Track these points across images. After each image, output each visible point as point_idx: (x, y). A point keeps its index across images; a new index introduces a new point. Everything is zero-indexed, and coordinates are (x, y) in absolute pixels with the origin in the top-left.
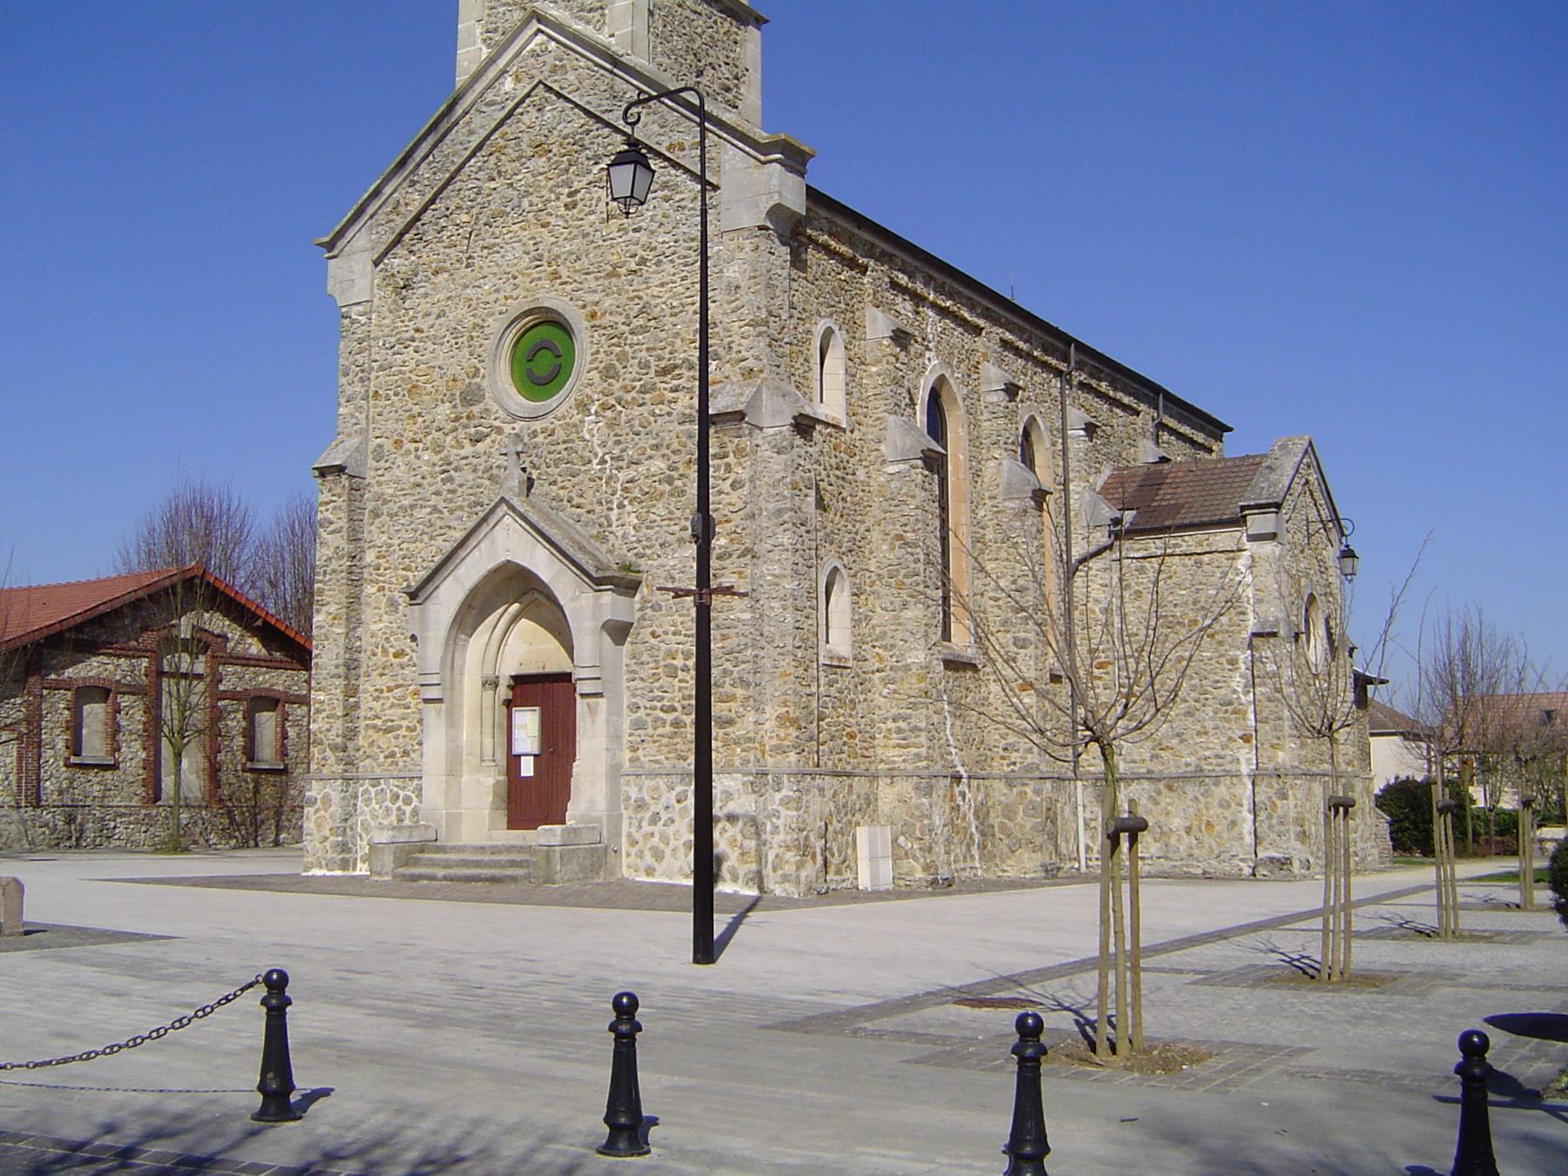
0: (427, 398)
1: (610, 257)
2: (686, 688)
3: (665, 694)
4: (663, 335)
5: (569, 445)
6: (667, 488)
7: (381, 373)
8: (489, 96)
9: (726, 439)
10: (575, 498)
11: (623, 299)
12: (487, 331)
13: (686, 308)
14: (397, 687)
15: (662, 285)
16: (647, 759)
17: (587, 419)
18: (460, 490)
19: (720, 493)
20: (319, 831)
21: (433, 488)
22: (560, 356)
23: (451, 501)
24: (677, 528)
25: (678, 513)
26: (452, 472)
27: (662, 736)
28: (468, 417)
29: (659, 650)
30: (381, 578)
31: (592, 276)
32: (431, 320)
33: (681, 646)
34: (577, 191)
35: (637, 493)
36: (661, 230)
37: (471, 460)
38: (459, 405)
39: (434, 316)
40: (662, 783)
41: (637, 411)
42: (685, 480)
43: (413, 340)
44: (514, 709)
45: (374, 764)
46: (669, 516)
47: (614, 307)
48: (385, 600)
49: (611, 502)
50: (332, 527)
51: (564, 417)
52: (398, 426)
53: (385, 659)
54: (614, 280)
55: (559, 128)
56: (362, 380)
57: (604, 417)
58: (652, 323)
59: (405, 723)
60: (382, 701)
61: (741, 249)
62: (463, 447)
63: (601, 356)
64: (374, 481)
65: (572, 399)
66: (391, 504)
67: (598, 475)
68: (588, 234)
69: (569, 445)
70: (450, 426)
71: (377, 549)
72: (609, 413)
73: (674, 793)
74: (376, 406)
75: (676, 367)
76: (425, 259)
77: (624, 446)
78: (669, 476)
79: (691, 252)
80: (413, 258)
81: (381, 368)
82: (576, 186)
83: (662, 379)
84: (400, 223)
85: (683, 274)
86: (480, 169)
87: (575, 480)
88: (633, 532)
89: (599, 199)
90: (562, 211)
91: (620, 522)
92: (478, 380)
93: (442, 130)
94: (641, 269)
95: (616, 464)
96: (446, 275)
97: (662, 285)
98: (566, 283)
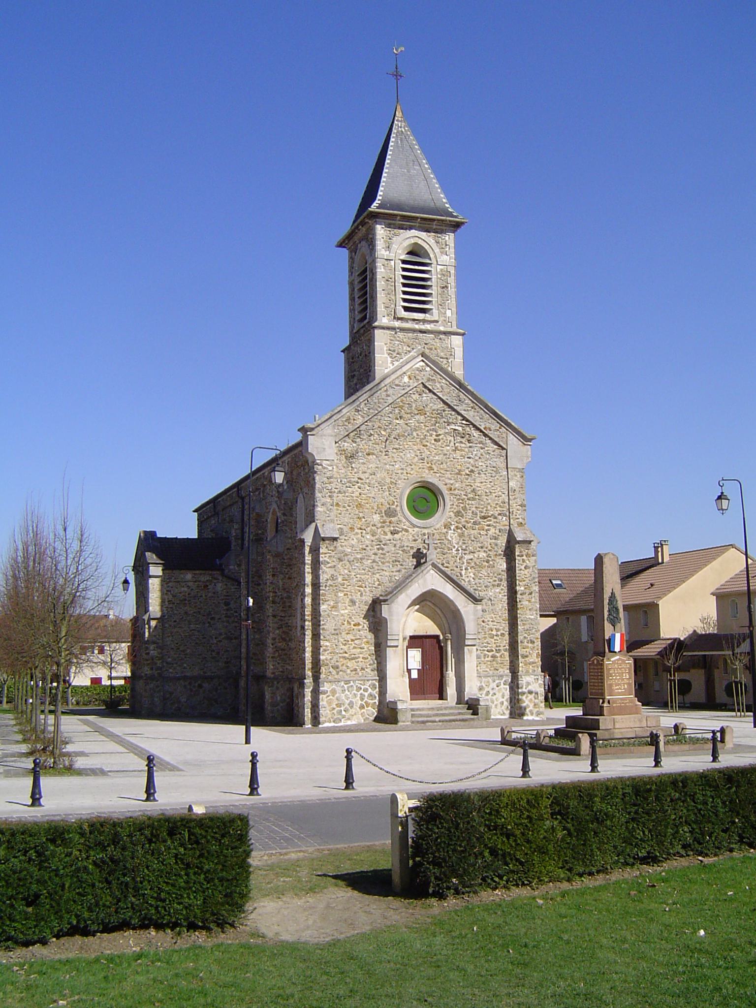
0: (366, 510)
4: (482, 503)
6: (487, 564)
8: (397, 382)
11: (464, 485)
14: (356, 639)
15: (482, 483)
19: (521, 570)
20: (329, 706)
21: (373, 552)
23: (383, 558)
25: (491, 575)
32: (367, 475)
34: (440, 435)
35: (473, 564)
40: (490, 680)
41: (473, 532)
50: (329, 565)
52: (351, 521)
54: (459, 476)
55: (431, 405)
56: (330, 496)
59: (361, 655)
60: (348, 646)
61: (516, 476)
63: (455, 506)
66: (349, 556)
68: (446, 454)
70: (380, 525)
72: (459, 531)
73: (495, 683)
74: (338, 510)
75: (489, 517)
76: (361, 446)
80: (354, 445)
82: (440, 433)
84: (351, 427)
86: (391, 413)
87: (445, 556)
89: (450, 441)
90: (433, 442)
92: (394, 507)
93: (373, 391)
96: (374, 457)
97: (482, 483)
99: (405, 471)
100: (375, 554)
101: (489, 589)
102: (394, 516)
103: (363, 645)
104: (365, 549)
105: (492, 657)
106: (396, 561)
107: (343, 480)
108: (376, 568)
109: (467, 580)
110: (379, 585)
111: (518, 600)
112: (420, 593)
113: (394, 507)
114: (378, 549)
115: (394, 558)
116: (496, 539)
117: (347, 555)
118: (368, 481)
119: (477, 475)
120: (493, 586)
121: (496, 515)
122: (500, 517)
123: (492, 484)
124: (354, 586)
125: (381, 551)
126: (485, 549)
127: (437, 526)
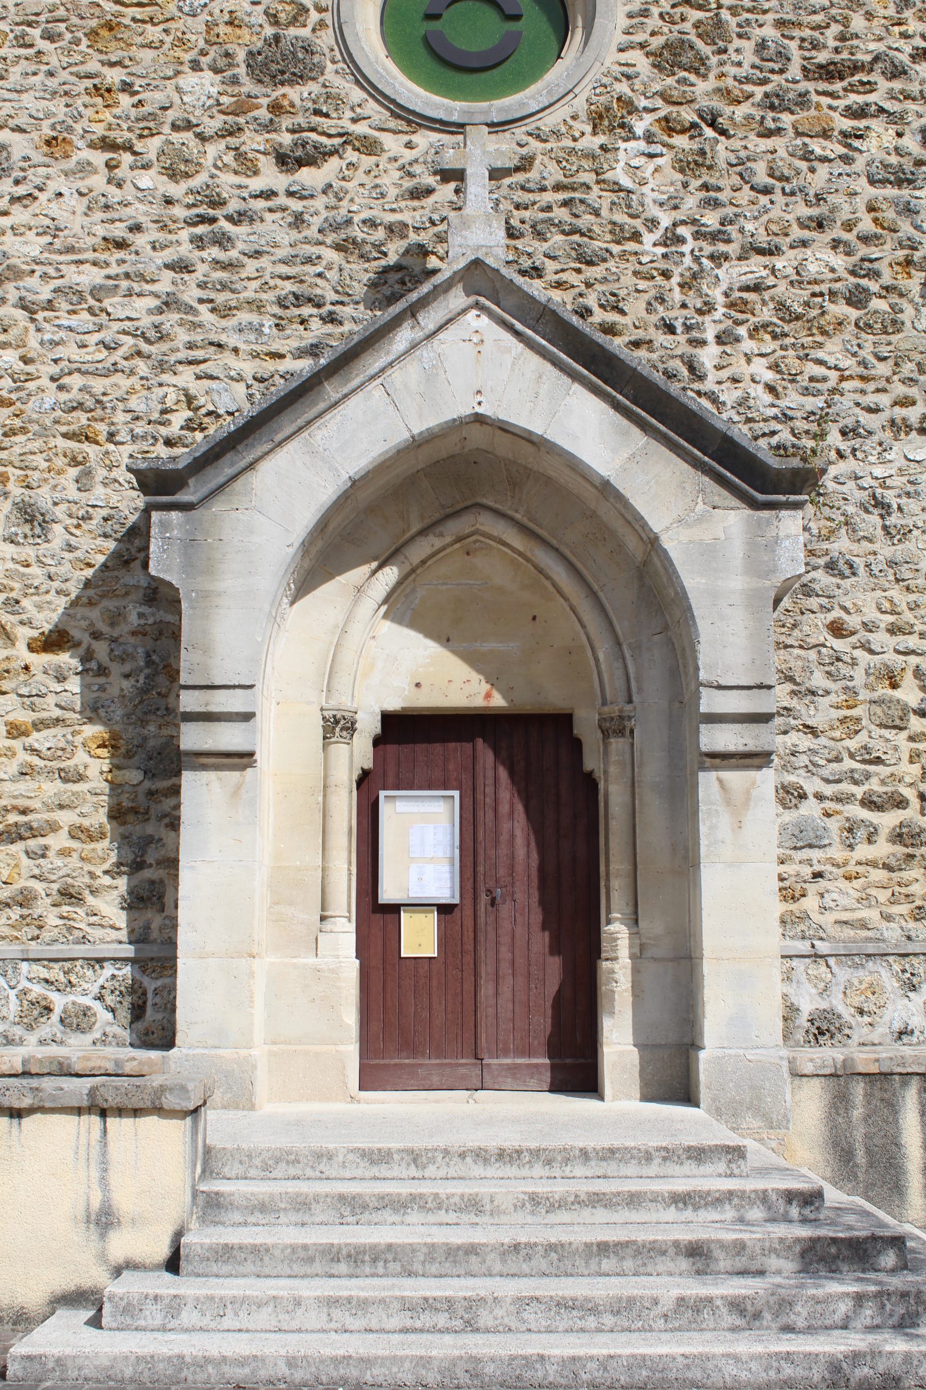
0: (148, 54)
3: (872, 768)
5: (577, 195)
6: (853, 314)
10: (596, 309)
14: (39, 725)
17: (622, 145)
18: (251, 266)
21: (168, 255)
22: (517, 17)
23: (224, 286)
24: (884, 400)
25: (883, 369)
26: (224, 224)
27: (873, 864)
28: (276, 108)
29: (854, 663)
37: (282, 200)
38: (244, 79)
42: (894, 299)
44: (382, 794)
46: (861, 370)
49: (699, 327)
51: (557, 134)
52: (58, 108)
59: (66, 818)
62: (256, 173)
63: (653, 22)
65: (582, 99)
66: (32, 282)
67: (662, 265)
69: (577, 195)
70: (212, 125)
72: (681, 141)
75: (856, 68)
77: (730, 211)
78: (857, 286)
83: (823, 86)
88: (768, 398)
91: (724, 374)
95: (708, 249)
100: (181, 267)
102: (300, 78)
103: (81, 757)
104: (121, 245)
105: (898, 837)
106: (299, 299)
108: (182, 336)
109: (729, 396)
110: (189, 426)
112: (401, 436)
113: (305, 32)
114: (199, 242)
115: (289, 287)
120: (898, 427)
121: (904, 58)
124: (44, 433)
125: (214, 252)
126: (837, 232)
127: (550, 121)
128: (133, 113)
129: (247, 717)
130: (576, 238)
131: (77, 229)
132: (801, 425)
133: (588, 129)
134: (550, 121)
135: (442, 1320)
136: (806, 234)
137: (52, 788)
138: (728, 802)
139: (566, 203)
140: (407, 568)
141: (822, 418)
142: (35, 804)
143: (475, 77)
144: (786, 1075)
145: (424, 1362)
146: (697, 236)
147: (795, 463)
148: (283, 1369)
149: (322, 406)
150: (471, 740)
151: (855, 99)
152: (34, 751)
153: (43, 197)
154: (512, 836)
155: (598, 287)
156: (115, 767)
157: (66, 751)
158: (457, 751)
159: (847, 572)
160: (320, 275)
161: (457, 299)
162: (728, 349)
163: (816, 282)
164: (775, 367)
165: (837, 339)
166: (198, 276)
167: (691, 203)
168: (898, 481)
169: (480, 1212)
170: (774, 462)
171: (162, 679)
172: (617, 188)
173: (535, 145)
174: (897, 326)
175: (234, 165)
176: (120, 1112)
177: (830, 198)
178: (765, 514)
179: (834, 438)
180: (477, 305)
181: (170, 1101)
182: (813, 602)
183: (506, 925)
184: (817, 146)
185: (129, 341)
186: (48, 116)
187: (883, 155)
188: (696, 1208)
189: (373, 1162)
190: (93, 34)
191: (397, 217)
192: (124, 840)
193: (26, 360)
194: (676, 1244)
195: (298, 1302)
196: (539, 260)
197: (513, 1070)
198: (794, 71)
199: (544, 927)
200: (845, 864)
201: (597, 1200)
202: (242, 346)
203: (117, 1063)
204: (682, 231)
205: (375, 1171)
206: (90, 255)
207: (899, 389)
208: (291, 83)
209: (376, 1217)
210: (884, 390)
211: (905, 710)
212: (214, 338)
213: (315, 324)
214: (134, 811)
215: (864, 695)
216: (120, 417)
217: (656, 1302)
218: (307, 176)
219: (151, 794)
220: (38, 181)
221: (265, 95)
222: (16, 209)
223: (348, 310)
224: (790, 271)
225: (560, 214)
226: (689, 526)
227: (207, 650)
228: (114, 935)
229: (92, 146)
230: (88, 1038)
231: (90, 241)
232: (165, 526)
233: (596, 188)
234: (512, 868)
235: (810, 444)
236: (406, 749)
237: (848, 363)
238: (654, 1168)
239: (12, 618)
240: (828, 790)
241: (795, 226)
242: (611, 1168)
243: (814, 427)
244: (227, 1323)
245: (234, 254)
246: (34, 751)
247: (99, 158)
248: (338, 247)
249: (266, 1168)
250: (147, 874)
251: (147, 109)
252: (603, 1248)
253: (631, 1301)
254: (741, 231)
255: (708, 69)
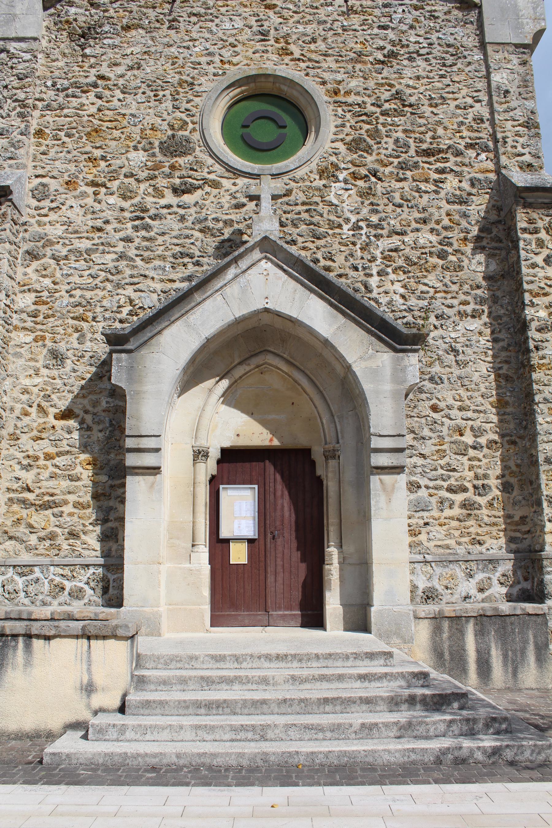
0: (114, 143)
1: (353, 45)
2: (480, 467)
3: (451, 473)
4: (422, 121)
5: (312, 207)
6: (441, 262)
7: (48, 112)
9: (535, 216)
10: (321, 259)
11: (371, 84)
12: (197, 88)
13: (448, 102)
14: (59, 454)
15: (418, 78)
16: (431, 544)
17: (333, 185)
18: (160, 240)
21: (122, 234)
22: (285, 127)
23: (148, 249)
24: (455, 302)
25: (455, 288)
27: (452, 518)
29: (443, 424)
30: (39, 327)
31: (332, 58)
32: (120, 70)
33: (470, 423)
35: (401, 262)
36: (413, 32)
37: (175, 209)
38: (158, 154)
39: (125, 67)
40: (459, 571)
42: (459, 256)
43: (95, 86)
45: (19, 546)
46: (444, 288)
47: (360, 89)
48: (45, 351)
49: (369, 268)
51: (303, 179)
52: (72, 168)
53: (41, 421)
54: (358, 66)
56: (21, 115)
57: (355, 186)
58: (406, 109)
59: (71, 498)
60: (35, 471)
62: (163, 197)
63: (347, 130)
64: (33, 221)
66: (58, 247)
67: (352, 239)
68: (325, 22)
69: (312, 207)
71: (34, 295)
72: (360, 183)
74: (39, 145)
75: (440, 151)
77: (383, 215)
78: (442, 250)
79: (448, 55)
81: (48, 107)
83: (425, 159)
85: (441, 73)
88: (401, 301)
91: (381, 290)
94: (391, 62)
95: (373, 232)
98: (299, 60)
99: (217, 59)
100: (128, 240)
101: (448, 322)
102: (184, 154)
103: (79, 469)
104: (100, 230)
105: (464, 505)
106: (183, 255)
107: (60, 82)
108: (128, 272)
109: (384, 300)
110: (130, 314)
111: (531, 344)
112: (230, 318)
113: (186, 133)
114: (136, 228)
115: (178, 249)
116: (462, 202)
117: (50, 243)
118: (121, 82)
119: (405, 62)
120: (462, 315)
121: (462, 147)
122: (472, 153)
123: (447, 81)
124: (63, 317)
125: (143, 233)
126: (433, 225)
127: (299, 173)
128: (106, 170)
129: (157, 450)
130: (312, 227)
131: (79, 223)
132: (417, 313)
133: (317, 177)
134: (299, 173)
135: (250, 735)
136: (418, 226)
137: (65, 484)
138: (384, 490)
139: (307, 211)
140: (233, 380)
141: (427, 310)
142: (57, 491)
143: (265, 153)
144: (412, 618)
145: (241, 755)
146: (368, 226)
147: (415, 331)
148: (174, 759)
149: (193, 304)
150: (263, 461)
151: (439, 165)
152: (57, 466)
153: (64, 208)
154: (283, 506)
155: (322, 249)
156: (95, 474)
157: (72, 466)
158: (257, 466)
159: (439, 382)
160: (192, 244)
161: (257, 254)
162: (383, 278)
163: (423, 248)
164: (405, 287)
165: (433, 274)
166: (136, 244)
167: (365, 211)
168: (462, 340)
169: (268, 684)
170: (405, 331)
171: (117, 433)
172: (331, 204)
173: (293, 184)
174: (461, 268)
175: (153, 193)
176: (97, 637)
177: (429, 209)
178: (401, 355)
179: (432, 319)
180: (266, 258)
181: (120, 632)
182: (424, 396)
183: (280, 549)
184: (423, 186)
185: (103, 274)
186: (67, 171)
187: (452, 191)
188: (370, 681)
189: (217, 661)
190: (88, 134)
191: (229, 217)
192: (99, 509)
193: (55, 283)
194: (361, 698)
195: (181, 727)
196: (295, 237)
197: (283, 617)
198: (412, 152)
199: (298, 550)
200: (439, 519)
201: (323, 678)
202: (156, 276)
203: (96, 614)
204: (361, 224)
205: (218, 665)
206: (85, 235)
207: (462, 297)
208: (180, 156)
209: (218, 687)
210: (455, 298)
211: (467, 446)
212: (143, 272)
213: (190, 266)
214: (104, 495)
215: (447, 439)
216: (98, 310)
217: (351, 726)
218: (187, 198)
219: (112, 487)
220: (62, 201)
221: (167, 161)
222: (51, 213)
223: (206, 260)
224: (411, 242)
225: (305, 216)
226: (365, 360)
227: (138, 419)
228: (94, 553)
229: (87, 184)
230: (82, 602)
231: (86, 228)
232: (119, 360)
233: (321, 204)
234: (282, 521)
235: (421, 322)
236: (232, 465)
237: (438, 285)
238: (350, 663)
239: (47, 404)
240: (431, 484)
241: (413, 222)
242: (330, 663)
243: (423, 315)
244: (148, 737)
245: (152, 234)
246: (57, 466)
247: (90, 190)
248: (201, 231)
249: (166, 664)
250: (110, 524)
251: (113, 168)
252: (326, 701)
253: (339, 725)
254: (389, 224)
255: (372, 151)
